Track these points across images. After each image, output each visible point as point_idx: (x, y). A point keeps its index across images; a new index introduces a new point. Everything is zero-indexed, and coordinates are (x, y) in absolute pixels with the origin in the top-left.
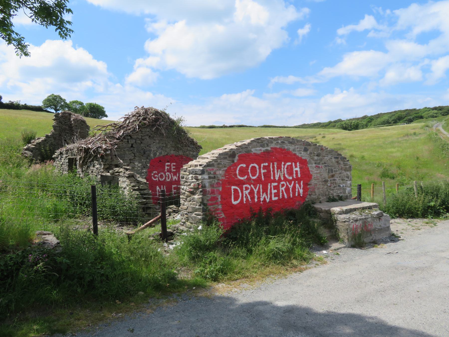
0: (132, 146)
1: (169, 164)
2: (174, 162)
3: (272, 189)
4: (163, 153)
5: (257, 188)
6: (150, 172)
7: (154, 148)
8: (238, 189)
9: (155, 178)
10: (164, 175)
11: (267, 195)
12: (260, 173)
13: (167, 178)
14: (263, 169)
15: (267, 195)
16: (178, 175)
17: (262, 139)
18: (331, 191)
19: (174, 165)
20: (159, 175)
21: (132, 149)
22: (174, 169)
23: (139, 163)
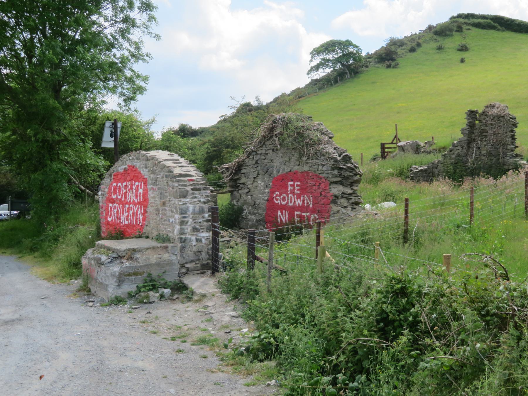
0: (257, 163)
1: (292, 183)
2: (298, 181)
4: (286, 169)
6: (272, 192)
7: (276, 164)
9: (277, 200)
10: (286, 198)
13: (289, 201)
16: (302, 198)
18: (162, 227)
19: (298, 185)
20: (282, 197)
21: (256, 166)
22: (298, 190)
23: (262, 182)
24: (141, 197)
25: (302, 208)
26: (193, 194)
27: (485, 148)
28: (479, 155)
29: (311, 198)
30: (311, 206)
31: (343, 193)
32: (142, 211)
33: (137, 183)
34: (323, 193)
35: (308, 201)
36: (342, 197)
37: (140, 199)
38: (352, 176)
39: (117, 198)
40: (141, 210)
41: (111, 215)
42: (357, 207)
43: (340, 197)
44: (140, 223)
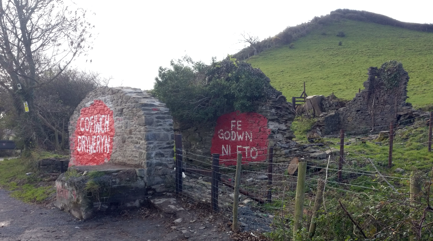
2: (240, 120)
9: (221, 136)
10: (229, 134)
20: (225, 133)
22: (239, 127)
24: (108, 128)
25: (244, 143)
26: (158, 122)
27: (383, 98)
28: (378, 104)
29: (251, 134)
30: (251, 140)
31: (279, 129)
32: (109, 140)
33: (103, 116)
34: (262, 129)
35: (249, 137)
36: (278, 133)
38: (287, 114)
39: (85, 130)
40: (108, 139)
41: (80, 146)
42: (290, 141)
43: (276, 133)
44: (107, 151)
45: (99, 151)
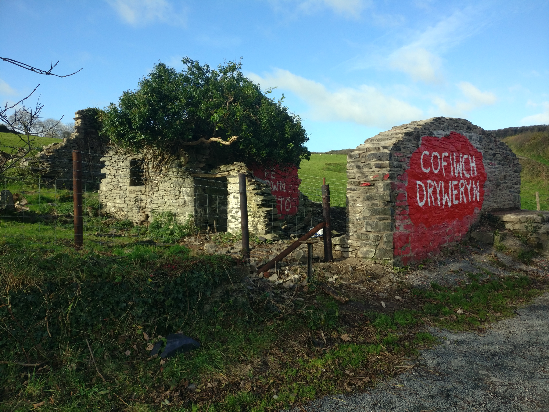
3: (453, 189)
5: (440, 186)
8: (423, 185)
11: (449, 196)
12: (441, 166)
14: (444, 161)
15: (449, 196)
17: (443, 119)
22: (274, 176)
24: (476, 172)
37: (474, 174)
39: (431, 172)
45: (463, 201)
